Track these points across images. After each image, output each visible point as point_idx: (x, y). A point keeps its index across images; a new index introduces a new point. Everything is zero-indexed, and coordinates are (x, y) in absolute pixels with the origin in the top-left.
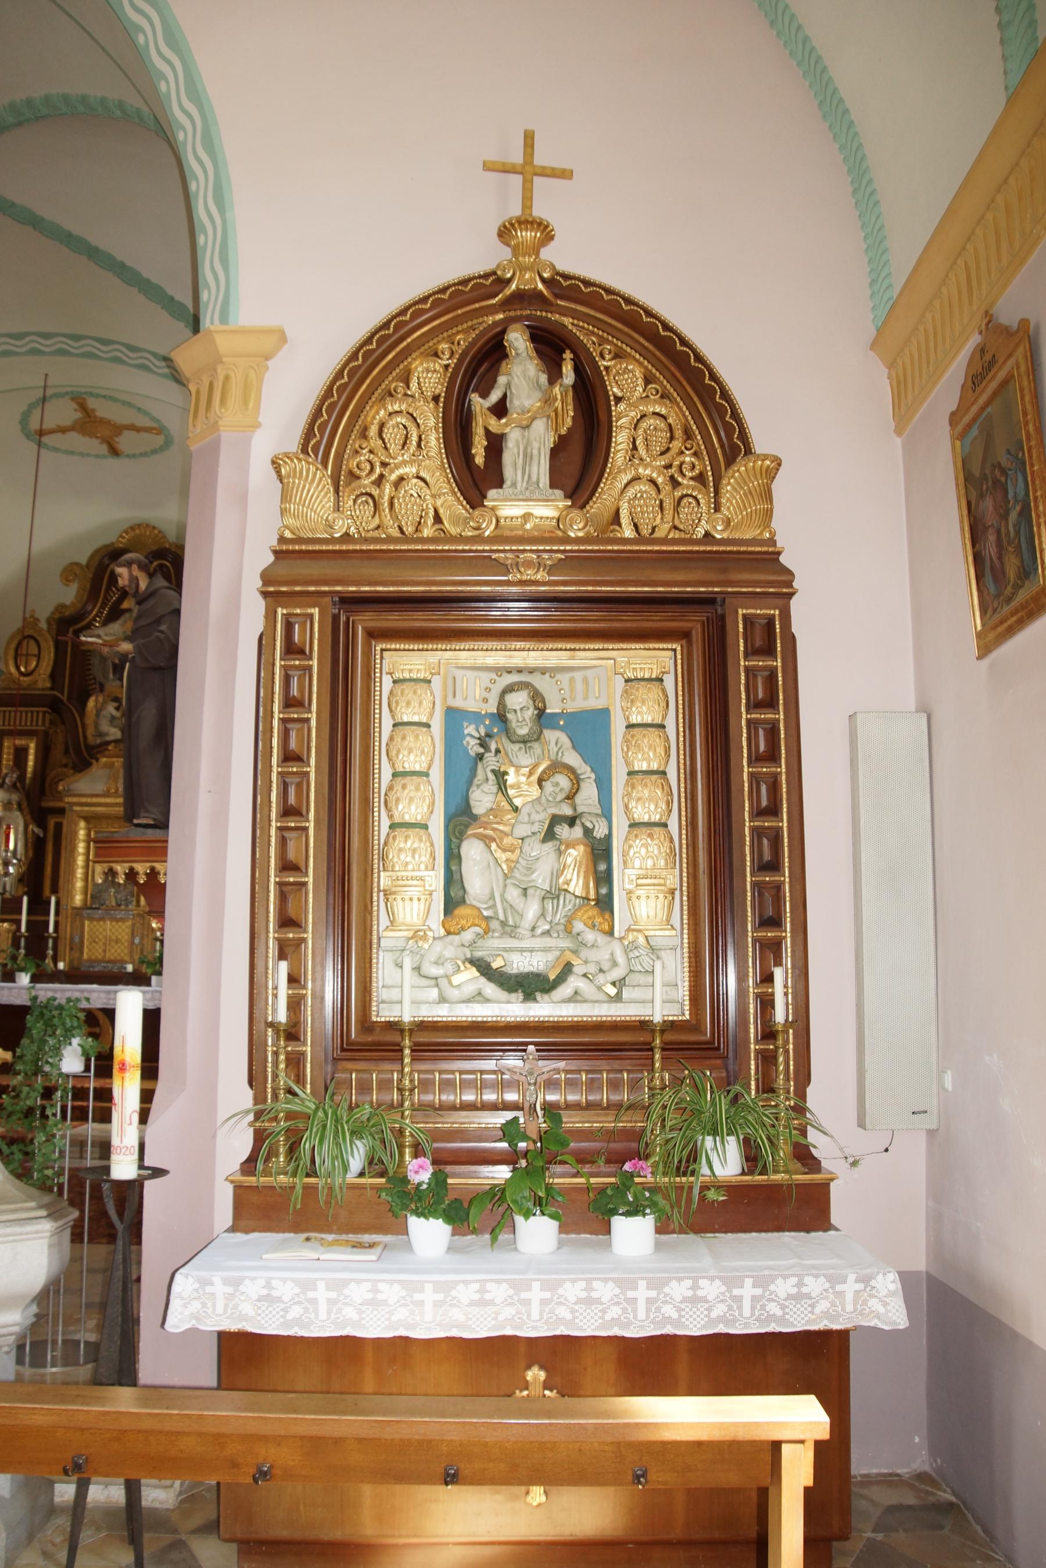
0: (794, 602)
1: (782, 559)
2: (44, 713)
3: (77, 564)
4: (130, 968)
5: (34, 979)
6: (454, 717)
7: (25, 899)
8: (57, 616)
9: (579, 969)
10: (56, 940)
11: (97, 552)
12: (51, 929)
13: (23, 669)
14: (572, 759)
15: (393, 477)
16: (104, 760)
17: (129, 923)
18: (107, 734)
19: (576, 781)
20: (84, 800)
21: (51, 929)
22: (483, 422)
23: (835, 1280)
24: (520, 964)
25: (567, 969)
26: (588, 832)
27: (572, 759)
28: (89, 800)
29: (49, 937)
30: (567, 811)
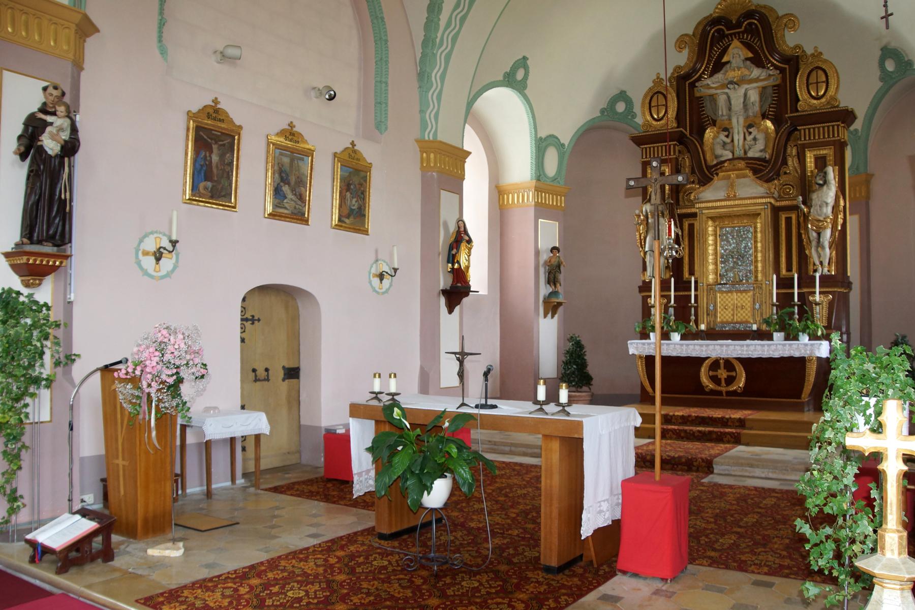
2: (674, 145)
3: (686, 35)
5: (683, 337)
7: (673, 279)
8: (676, 75)
10: (696, 308)
11: (699, 24)
12: (693, 301)
13: (656, 117)
16: (721, 174)
17: (751, 294)
18: (721, 156)
20: (710, 205)
21: (693, 301)
28: (714, 204)
29: (691, 307)
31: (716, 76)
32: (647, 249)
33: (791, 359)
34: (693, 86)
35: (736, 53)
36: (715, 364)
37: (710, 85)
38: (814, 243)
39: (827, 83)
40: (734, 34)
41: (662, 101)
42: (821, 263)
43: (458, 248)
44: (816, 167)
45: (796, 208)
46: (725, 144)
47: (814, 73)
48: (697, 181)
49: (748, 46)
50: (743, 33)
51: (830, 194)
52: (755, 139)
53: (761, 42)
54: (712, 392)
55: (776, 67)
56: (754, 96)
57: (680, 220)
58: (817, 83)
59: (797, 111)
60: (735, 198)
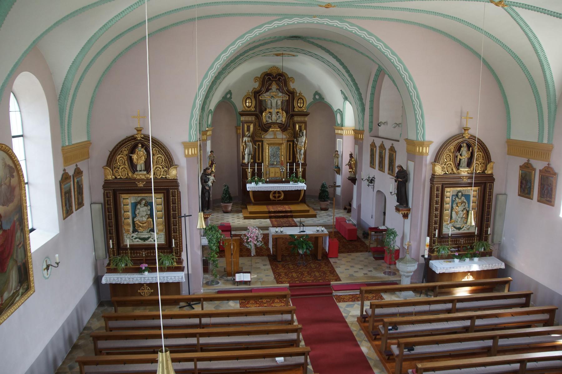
0: (494, 182)
1: (494, 176)
3: (258, 77)
4: (284, 180)
6: (453, 196)
9: (465, 226)
14: (465, 200)
15: (447, 164)
19: (465, 203)
22: (459, 157)
23: (499, 264)
24: (458, 226)
25: (463, 227)
26: (466, 210)
27: (465, 200)
30: (464, 207)
31: (267, 93)
32: (246, 153)
33: (298, 190)
34: (259, 95)
35: (274, 87)
36: (275, 192)
37: (265, 97)
38: (298, 153)
39: (303, 103)
40: (274, 80)
41: (250, 101)
42: (300, 159)
43: (212, 166)
44: (299, 129)
45: (293, 142)
46: (269, 117)
47: (300, 100)
48: (260, 129)
49: (278, 85)
50: (277, 80)
51: (304, 139)
52: (279, 117)
53: (282, 85)
54: (274, 200)
55: (287, 94)
56: (279, 103)
57: (254, 141)
58: (301, 103)
59: (294, 111)
60: (276, 138)
